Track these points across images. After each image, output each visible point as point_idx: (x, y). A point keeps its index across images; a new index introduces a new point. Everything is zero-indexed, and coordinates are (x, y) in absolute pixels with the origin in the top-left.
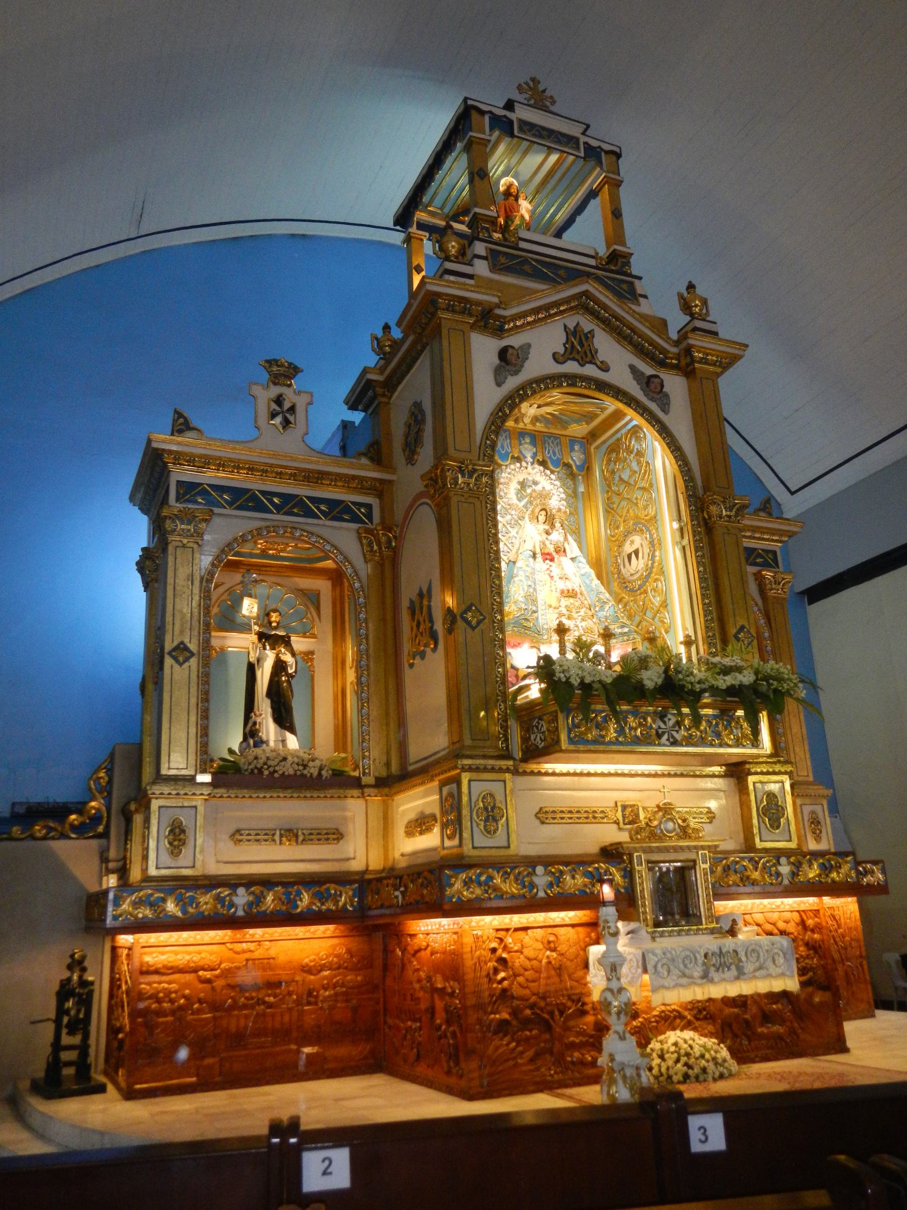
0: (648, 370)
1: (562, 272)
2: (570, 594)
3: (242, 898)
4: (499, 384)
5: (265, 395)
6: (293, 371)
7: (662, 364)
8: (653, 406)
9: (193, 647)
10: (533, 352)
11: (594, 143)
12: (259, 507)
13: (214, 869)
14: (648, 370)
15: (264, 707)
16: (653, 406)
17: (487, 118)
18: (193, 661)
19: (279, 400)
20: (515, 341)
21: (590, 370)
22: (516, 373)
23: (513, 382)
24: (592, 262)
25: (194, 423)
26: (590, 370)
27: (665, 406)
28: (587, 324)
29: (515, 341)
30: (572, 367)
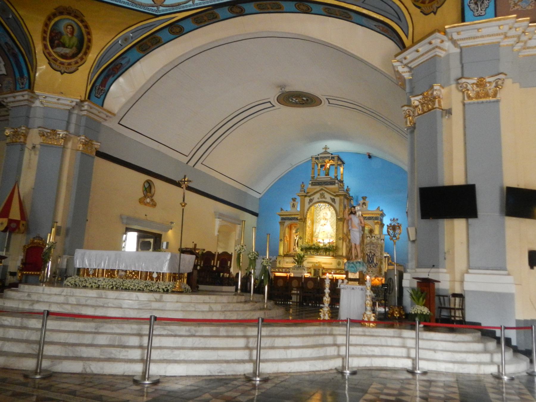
0: (333, 197)
1: (323, 183)
2: (324, 232)
3: (284, 270)
4: (309, 204)
5: (292, 204)
6: (296, 198)
7: (335, 196)
8: (333, 204)
9: (283, 239)
10: (315, 199)
11: (333, 156)
12: (291, 220)
13: (284, 266)
14: (333, 197)
15: (296, 245)
16: (333, 204)
17: (315, 159)
18: (283, 241)
19: (293, 204)
20: (312, 198)
21: (324, 200)
22: (311, 202)
23: (311, 204)
24: (329, 179)
25: (283, 209)
26: (324, 200)
27: (335, 202)
28: (323, 192)
29: (312, 198)
30: (321, 200)
